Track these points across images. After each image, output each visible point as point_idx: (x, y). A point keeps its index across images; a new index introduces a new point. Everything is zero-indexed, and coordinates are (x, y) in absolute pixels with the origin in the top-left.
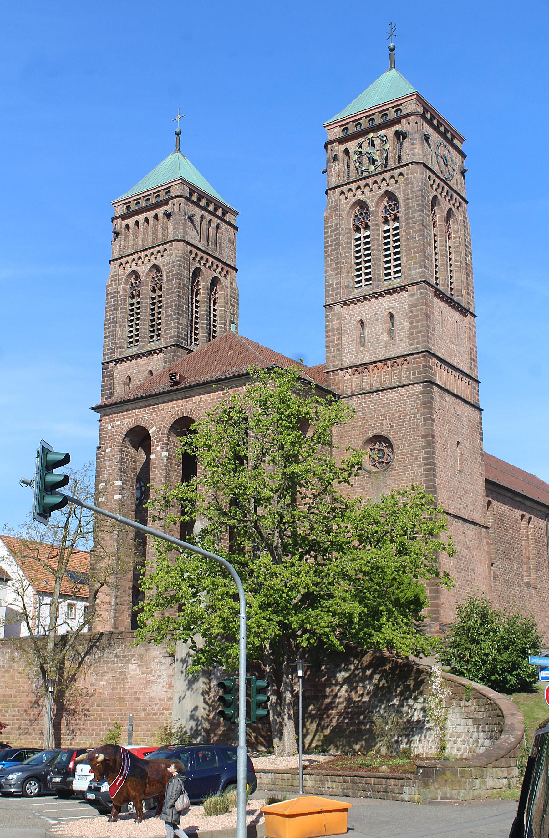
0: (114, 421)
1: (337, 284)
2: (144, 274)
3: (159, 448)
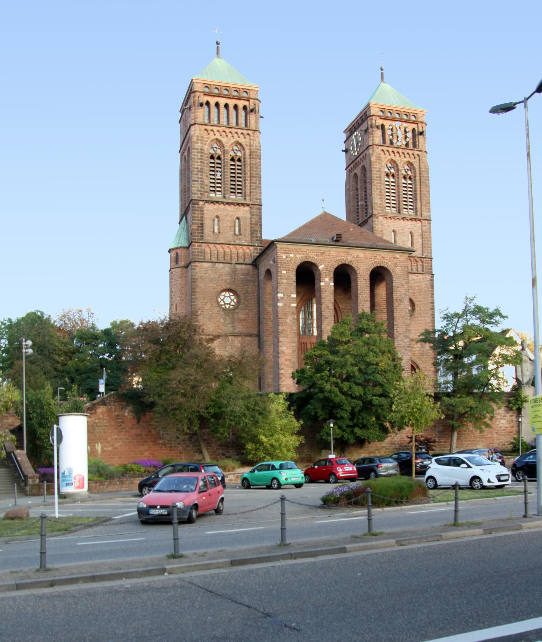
0: (288, 253)
1: (380, 204)
2: (228, 145)
3: (327, 279)
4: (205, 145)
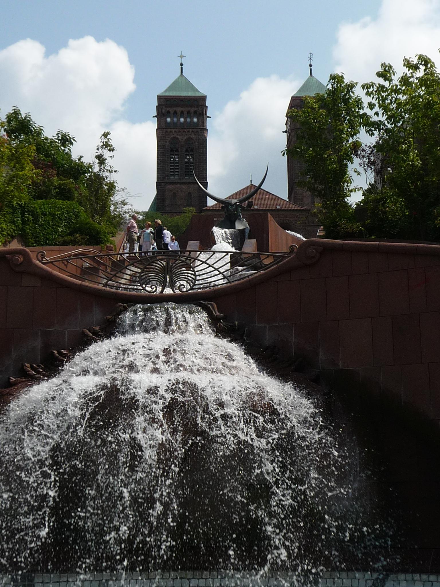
4: (166, 142)
